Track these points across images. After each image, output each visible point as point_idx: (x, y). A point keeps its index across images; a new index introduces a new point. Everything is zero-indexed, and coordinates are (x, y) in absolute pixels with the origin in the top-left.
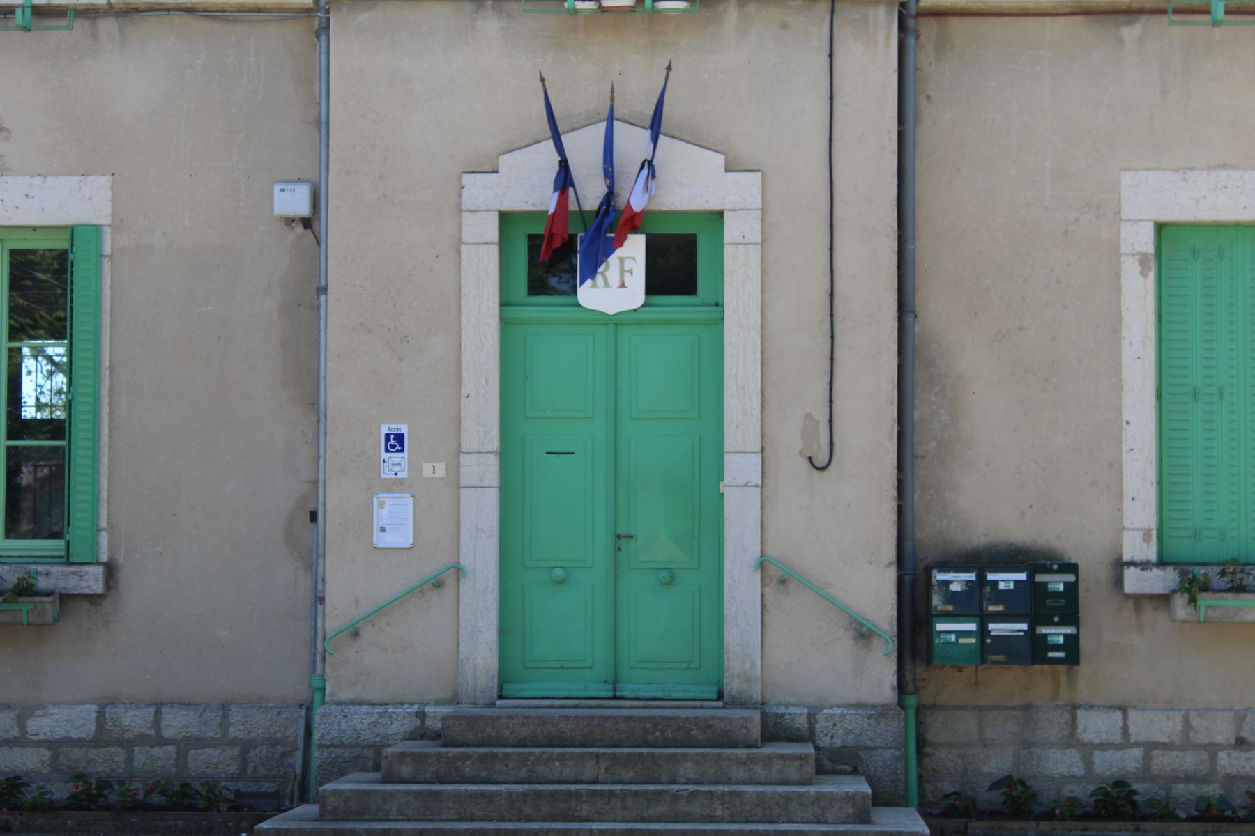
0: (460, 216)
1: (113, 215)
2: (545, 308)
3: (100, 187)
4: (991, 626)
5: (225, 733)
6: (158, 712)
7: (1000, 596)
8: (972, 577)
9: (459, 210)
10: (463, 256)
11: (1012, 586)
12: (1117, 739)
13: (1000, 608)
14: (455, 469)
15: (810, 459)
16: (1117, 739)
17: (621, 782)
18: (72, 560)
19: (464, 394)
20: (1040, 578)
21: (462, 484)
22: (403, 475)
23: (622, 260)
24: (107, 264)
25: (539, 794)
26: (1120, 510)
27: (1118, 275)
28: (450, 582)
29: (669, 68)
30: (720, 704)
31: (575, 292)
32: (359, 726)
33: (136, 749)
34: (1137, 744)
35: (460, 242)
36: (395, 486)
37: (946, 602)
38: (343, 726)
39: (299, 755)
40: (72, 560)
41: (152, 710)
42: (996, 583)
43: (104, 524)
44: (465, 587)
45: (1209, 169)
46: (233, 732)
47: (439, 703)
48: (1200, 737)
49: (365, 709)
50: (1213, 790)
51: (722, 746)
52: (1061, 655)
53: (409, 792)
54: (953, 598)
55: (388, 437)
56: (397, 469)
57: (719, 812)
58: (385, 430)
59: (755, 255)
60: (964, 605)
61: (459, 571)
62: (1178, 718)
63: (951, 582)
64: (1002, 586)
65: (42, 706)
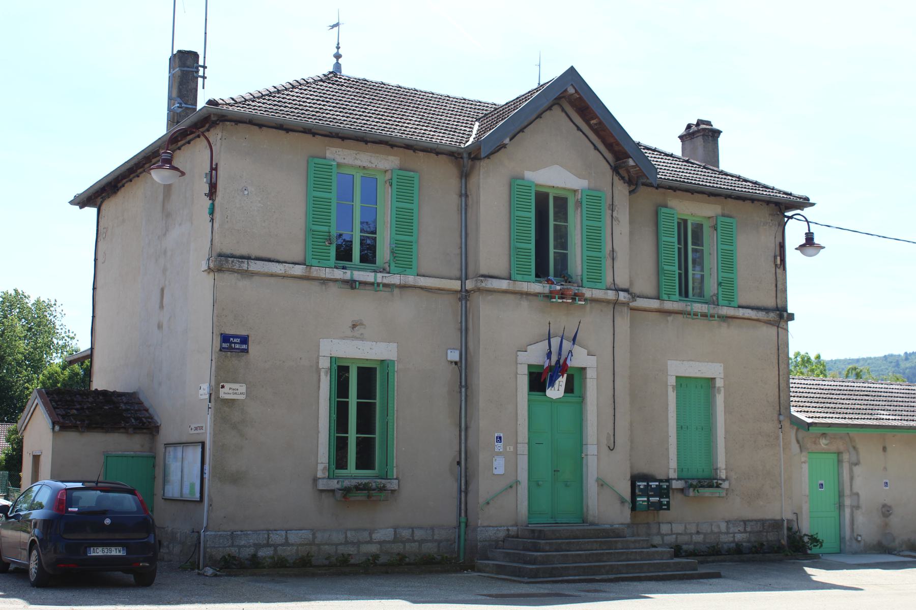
0: (517, 365)
1: (398, 357)
2: (537, 396)
3: (394, 346)
4: (650, 499)
5: (433, 538)
6: (413, 531)
7: (652, 490)
8: (645, 484)
9: (517, 364)
10: (518, 378)
11: (655, 486)
12: (670, 532)
13: (652, 493)
14: (516, 448)
15: (609, 447)
16: (670, 532)
17: (603, 550)
18: (388, 478)
19: (518, 423)
20: (661, 484)
21: (518, 453)
22: (501, 450)
23: (559, 382)
24: (396, 374)
25: (593, 554)
26: (669, 463)
27: (667, 391)
28: (514, 486)
29: (580, 322)
30: (588, 525)
31: (544, 391)
32: (491, 534)
33: (406, 544)
34: (674, 534)
35: (517, 373)
36: (499, 454)
37: (639, 492)
38: (486, 534)
39: (457, 544)
40: (388, 478)
41: (411, 530)
42: (651, 485)
43: (395, 465)
44: (519, 488)
45: (688, 361)
46: (436, 537)
47: (512, 526)
48: (688, 531)
49: (491, 528)
50: (691, 547)
51: (617, 538)
52: (666, 507)
53: (559, 555)
54: (641, 490)
55: (497, 437)
56: (499, 448)
57: (638, 558)
58: (496, 435)
59: (595, 381)
60: (646, 492)
61: (517, 482)
62: (683, 525)
63: (640, 485)
64: (653, 486)
65: (376, 530)
